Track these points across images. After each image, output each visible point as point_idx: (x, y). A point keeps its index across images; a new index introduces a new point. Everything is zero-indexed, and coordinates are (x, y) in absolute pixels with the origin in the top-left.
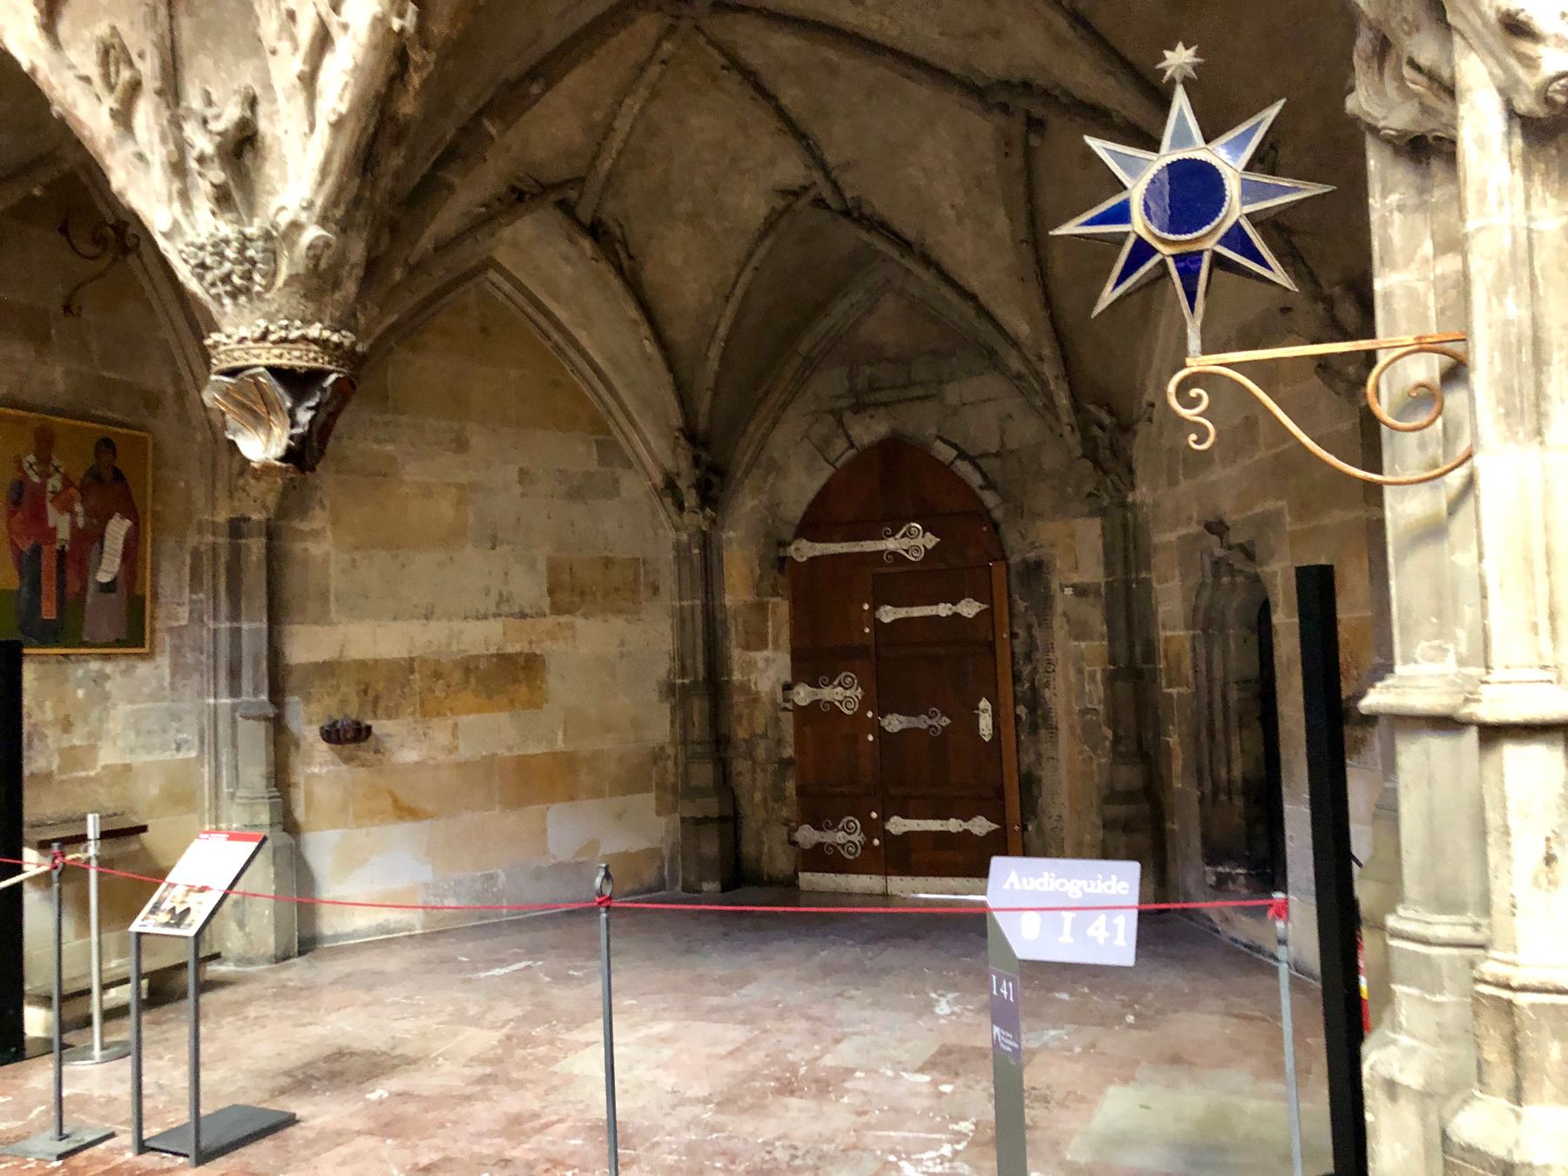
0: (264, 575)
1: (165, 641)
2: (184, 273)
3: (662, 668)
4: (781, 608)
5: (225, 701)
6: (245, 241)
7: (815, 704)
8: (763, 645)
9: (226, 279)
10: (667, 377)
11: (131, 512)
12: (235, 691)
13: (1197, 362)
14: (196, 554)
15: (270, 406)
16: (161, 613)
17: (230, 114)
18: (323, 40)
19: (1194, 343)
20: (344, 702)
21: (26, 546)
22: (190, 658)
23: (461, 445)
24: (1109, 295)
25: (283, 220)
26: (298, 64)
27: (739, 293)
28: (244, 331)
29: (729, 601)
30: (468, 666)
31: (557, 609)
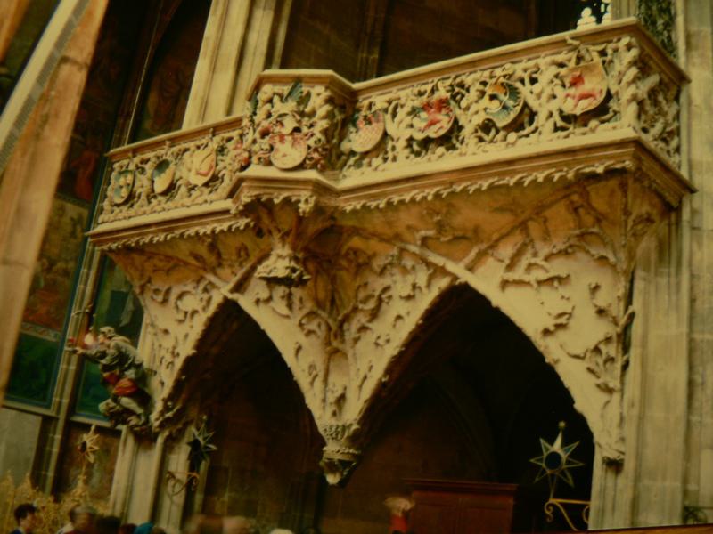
9: (331, 435)
17: (340, 392)
25: (348, 423)
26: (358, 383)
28: (333, 449)
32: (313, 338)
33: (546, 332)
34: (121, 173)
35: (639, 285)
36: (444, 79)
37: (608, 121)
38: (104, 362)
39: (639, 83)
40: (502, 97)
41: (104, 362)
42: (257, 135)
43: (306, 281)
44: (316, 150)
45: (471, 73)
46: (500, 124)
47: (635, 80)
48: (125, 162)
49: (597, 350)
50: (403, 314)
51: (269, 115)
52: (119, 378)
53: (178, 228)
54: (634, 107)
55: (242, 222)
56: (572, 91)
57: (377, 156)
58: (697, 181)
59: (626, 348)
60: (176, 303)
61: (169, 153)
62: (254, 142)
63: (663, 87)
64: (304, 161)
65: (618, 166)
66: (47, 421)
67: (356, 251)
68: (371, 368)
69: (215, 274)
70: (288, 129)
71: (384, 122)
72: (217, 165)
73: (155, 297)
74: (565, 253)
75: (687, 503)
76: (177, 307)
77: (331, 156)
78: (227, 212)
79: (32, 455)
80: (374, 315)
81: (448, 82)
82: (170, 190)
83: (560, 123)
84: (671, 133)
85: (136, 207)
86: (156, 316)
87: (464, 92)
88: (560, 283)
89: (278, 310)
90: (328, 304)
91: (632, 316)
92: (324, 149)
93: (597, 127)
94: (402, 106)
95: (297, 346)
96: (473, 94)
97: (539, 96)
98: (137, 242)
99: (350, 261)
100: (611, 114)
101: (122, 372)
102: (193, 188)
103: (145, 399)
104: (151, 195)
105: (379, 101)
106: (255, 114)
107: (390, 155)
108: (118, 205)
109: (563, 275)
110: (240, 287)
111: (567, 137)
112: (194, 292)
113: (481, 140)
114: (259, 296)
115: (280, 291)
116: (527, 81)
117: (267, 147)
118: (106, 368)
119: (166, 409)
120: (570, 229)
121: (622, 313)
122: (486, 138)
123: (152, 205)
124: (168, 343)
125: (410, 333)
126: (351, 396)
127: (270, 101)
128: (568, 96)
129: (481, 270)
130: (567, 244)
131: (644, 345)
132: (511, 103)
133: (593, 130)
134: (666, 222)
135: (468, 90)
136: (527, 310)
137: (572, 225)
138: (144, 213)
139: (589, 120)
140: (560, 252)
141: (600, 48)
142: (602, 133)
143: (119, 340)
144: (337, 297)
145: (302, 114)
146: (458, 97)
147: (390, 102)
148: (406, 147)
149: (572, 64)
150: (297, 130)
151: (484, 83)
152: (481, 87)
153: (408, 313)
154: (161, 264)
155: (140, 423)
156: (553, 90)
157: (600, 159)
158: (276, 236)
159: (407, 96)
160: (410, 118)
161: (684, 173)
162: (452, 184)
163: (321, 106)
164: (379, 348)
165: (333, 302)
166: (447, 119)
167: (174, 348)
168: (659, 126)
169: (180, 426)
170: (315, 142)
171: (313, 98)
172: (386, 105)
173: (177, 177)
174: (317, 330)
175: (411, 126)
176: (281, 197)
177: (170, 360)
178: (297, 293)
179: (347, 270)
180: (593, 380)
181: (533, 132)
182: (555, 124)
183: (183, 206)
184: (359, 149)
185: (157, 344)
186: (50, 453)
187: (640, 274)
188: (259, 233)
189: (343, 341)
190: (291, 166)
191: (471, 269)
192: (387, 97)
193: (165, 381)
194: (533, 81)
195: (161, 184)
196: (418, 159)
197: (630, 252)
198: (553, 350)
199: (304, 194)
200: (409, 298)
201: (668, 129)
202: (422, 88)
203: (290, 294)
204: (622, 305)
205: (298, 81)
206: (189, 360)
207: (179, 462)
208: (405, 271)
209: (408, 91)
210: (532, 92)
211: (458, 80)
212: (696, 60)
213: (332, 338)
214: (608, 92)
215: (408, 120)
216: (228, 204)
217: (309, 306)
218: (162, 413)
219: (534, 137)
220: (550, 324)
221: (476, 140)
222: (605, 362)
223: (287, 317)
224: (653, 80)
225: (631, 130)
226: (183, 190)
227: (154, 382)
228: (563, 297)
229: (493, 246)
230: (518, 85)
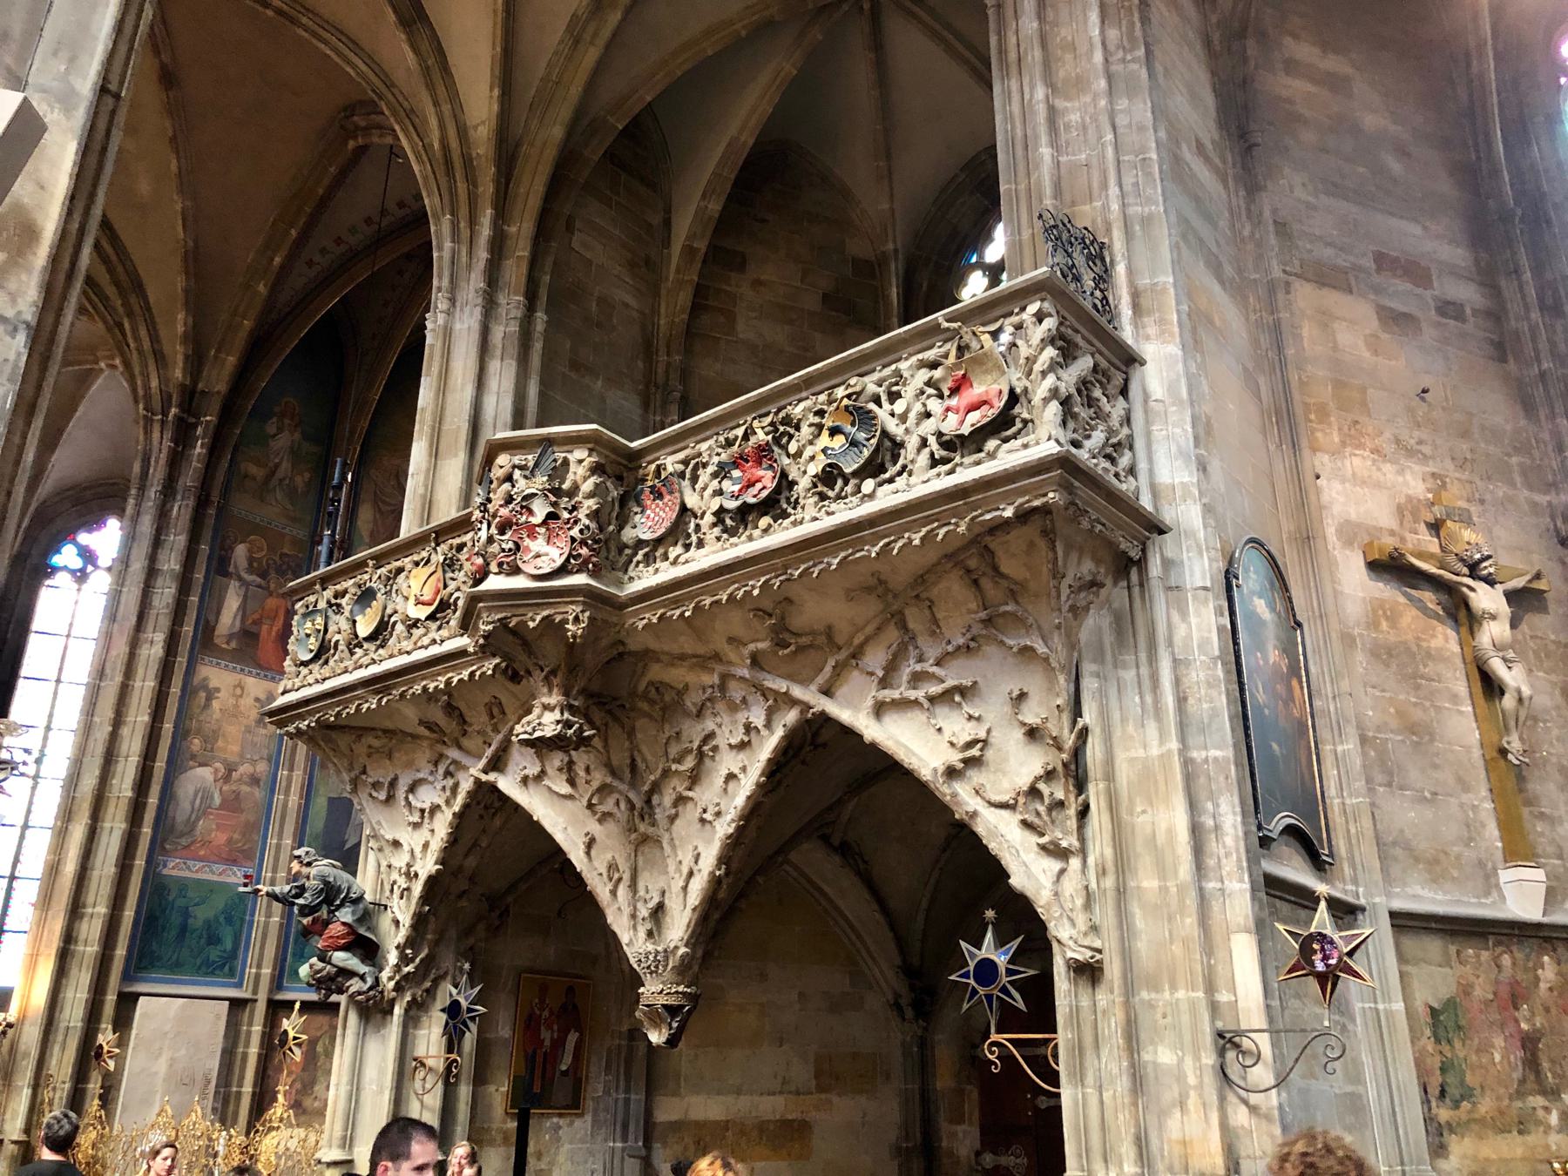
0: (648, 1072)
1: (590, 1104)
2: (633, 961)
3: (893, 1135)
4: (974, 1094)
5: (619, 1145)
6: (657, 952)
7: (997, 1168)
8: (961, 1121)
10: (891, 935)
11: (579, 1029)
12: (625, 1139)
13: (994, 1037)
14: (609, 1051)
15: (662, 1020)
16: (589, 1088)
18: (691, 874)
19: (993, 1030)
20: (686, 1149)
21: (530, 1052)
22: (602, 1116)
23: (763, 977)
24: (965, 1006)
25: (672, 945)
26: (681, 883)
27: (932, 881)
29: (939, 1085)
30: (762, 1127)
31: (821, 1089)
32: (611, 825)
33: (951, 773)
34: (305, 616)
35: (1089, 685)
36: (761, 416)
37: (1015, 437)
38: (301, 901)
39: (1060, 371)
40: (848, 428)
41: (301, 901)
42: (494, 531)
43: (590, 738)
44: (583, 543)
45: (800, 401)
46: (848, 470)
47: (1053, 366)
48: (312, 599)
49: (1033, 792)
50: (736, 771)
51: (509, 499)
52: (327, 923)
53: (395, 686)
54: (1054, 407)
55: (489, 666)
56: (954, 402)
57: (676, 544)
58: (1167, 516)
59: (1081, 787)
60: (407, 798)
61: (375, 577)
62: (490, 540)
63: (1100, 377)
64: (567, 560)
65: (1036, 503)
66: (237, 1005)
67: (659, 687)
68: (697, 858)
69: (460, 748)
70: (538, 518)
71: (681, 492)
72: (445, 586)
73: (375, 794)
74: (967, 650)
75: (1220, 1025)
76: (409, 804)
77: (606, 549)
78: (462, 653)
79: (214, 1064)
80: (694, 778)
81: (769, 419)
82: (380, 633)
83: (940, 453)
84: (1118, 446)
85: (331, 662)
86: (379, 823)
87: (792, 431)
88: (963, 695)
89: (555, 788)
90: (627, 771)
91: (1084, 733)
92: (596, 541)
93: (999, 447)
94: (705, 465)
95: (587, 840)
96: (806, 431)
97: (903, 418)
98: (339, 714)
99: (652, 702)
100: (1019, 425)
101: (331, 912)
102: (415, 624)
103: (369, 950)
104: (354, 643)
105: (671, 463)
106: (489, 500)
107: (694, 538)
108: (305, 664)
109: (967, 682)
110: (497, 763)
111: (951, 472)
112: (431, 778)
113: (823, 497)
114: (526, 772)
115: (557, 759)
116: (884, 398)
117: (511, 545)
118: (306, 910)
119: (404, 960)
120: (970, 612)
121: (1066, 731)
122: (831, 494)
123: (355, 657)
124: (400, 860)
125: (749, 798)
126: (673, 904)
127: (509, 478)
128: (948, 409)
129: (842, 691)
130: (968, 636)
131: (1110, 777)
132: (862, 436)
133: (992, 456)
134: (1125, 584)
135: (798, 428)
136: (919, 743)
137: (973, 606)
138: (346, 671)
139: (985, 440)
140: (959, 648)
141: (992, 328)
142: (1008, 456)
143: (324, 867)
144: (639, 760)
145: (557, 492)
146: (784, 440)
147: (686, 462)
148: (714, 525)
149: (952, 359)
150: (552, 516)
151: (820, 413)
152: (817, 420)
153: (744, 769)
154: (376, 743)
155: (365, 988)
156: (924, 405)
157: (1008, 498)
158: (538, 676)
159: (710, 448)
160: (715, 482)
161: (1146, 502)
162: (786, 567)
163: (585, 479)
164: (708, 826)
165: (633, 767)
166: (770, 474)
167: (409, 866)
168: (1098, 437)
169: (428, 984)
170: (581, 531)
171: (573, 468)
172: (681, 467)
173: (389, 611)
174: (615, 810)
175: (719, 492)
176: (538, 618)
177: (405, 886)
178: (581, 758)
179: (650, 717)
180: (1034, 839)
181: (900, 474)
182: (932, 454)
183: (401, 653)
184: (647, 536)
185: (384, 863)
186: (245, 1056)
187: (1088, 668)
188: (515, 677)
189: (654, 824)
190: (547, 570)
191: (827, 692)
192: (681, 456)
193: (400, 918)
194: (894, 397)
195: (364, 628)
196: (734, 540)
197: (1068, 636)
198: (964, 797)
199: (573, 610)
200: (743, 746)
201: (1114, 440)
202: (731, 436)
203: (570, 765)
204: (1066, 718)
205: (549, 442)
206: (432, 881)
207: (430, 1041)
208: (733, 708)
209: (711, 442)
210: (893, 415)
211: (781, 415)
212: (1152, 330)
213: (637, 821)
214: (1012, 391)
215: (715, 484)
216: (463, 641)
217: (599, 777)
218: (398, 968)
219: (901, 482)
220: (955, 758)
221: (816, 498)
222: (1050, 809)
223: (570, 797)
224: (1084, 364)
225: (1052, 442)
226: (400, 628)
227: (385, 922)
228: (970, 717)
229: (856, 655)
230: (872, 406)
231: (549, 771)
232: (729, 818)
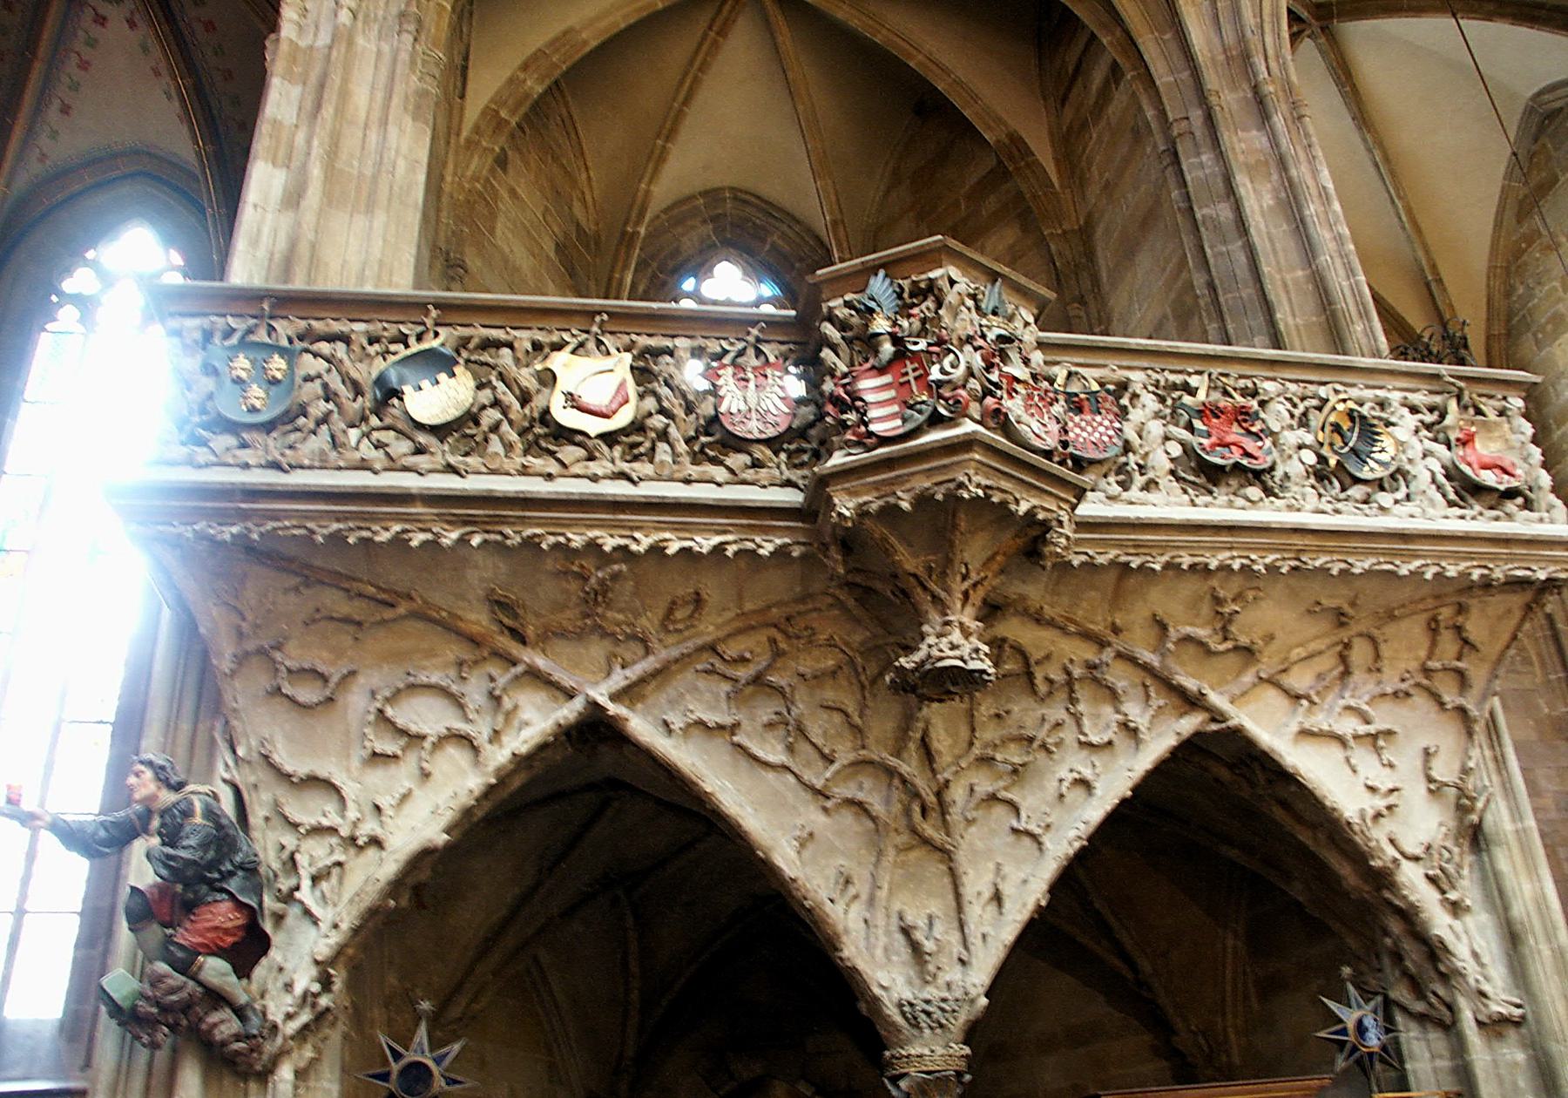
32: (847, 818)
111: (1497, 519)
164: (1027, 841)
231: (745, 724)
232: (1072, 834)
